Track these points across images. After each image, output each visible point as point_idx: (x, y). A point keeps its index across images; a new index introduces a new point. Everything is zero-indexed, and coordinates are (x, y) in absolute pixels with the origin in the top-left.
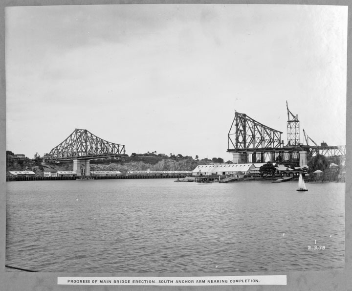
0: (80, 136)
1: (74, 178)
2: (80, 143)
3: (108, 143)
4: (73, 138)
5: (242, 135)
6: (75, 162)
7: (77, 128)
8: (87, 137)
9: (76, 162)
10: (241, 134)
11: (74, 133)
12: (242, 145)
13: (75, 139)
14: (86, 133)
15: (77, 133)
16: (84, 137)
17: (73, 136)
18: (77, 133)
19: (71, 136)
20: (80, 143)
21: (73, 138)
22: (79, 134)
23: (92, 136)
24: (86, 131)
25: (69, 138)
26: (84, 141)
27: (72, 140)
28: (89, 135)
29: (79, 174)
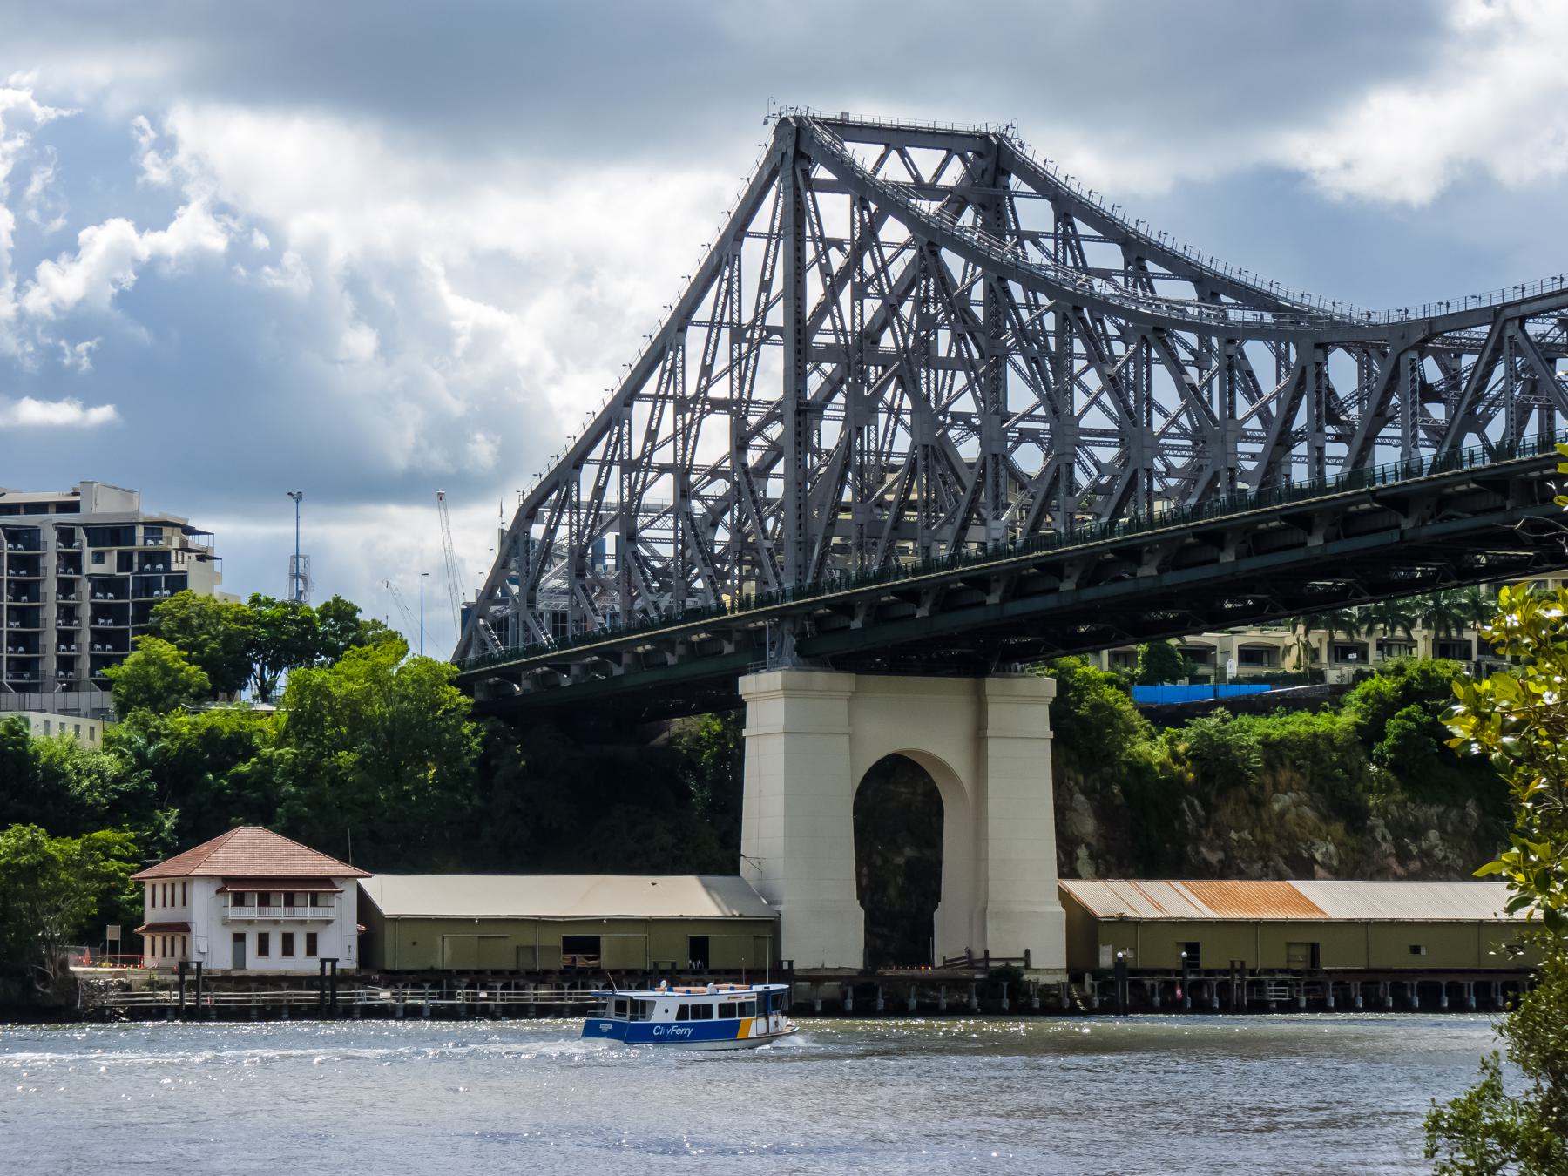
11: (763, 220)
19: (723, 258)
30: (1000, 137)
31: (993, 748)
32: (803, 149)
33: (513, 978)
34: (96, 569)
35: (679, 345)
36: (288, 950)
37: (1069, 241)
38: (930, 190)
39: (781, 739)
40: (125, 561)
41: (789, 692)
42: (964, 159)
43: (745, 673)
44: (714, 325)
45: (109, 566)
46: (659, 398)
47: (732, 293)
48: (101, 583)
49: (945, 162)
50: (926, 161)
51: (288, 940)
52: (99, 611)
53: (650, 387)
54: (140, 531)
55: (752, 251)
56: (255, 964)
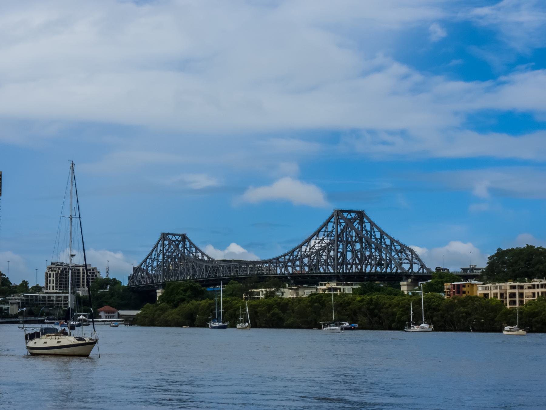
7: (166, 232)
11: (160, 243)
19: (156, 247)
25: (154, 251)
30: (185, 234)
35: (152, 254)
38: (177, 240)
42: (181, 237)
46: (150, 259)
47: (157, 250)
49: (179, 237)
50: (177, 237)
53: (149, 258)
55: (159, 245)
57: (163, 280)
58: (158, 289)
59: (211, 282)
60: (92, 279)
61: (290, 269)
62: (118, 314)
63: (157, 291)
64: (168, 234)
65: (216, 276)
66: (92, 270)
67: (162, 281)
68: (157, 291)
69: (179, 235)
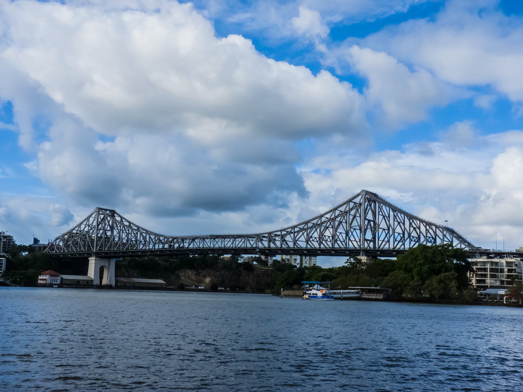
0: (103, 220)
1: (88, 285)
2: (101, 232)
3: (147, 232)
4: (91, 222)
5: (371, 228)
6: (92, 261)
8: (115, 221)
9: (94, 261)
10: (369, 227)
11: (94, 216)
12: (372, 244)
13: (95, 224)
14: (113, 216)
15: (99, 214)
16: (109, 222)
17: (91, 219)
18: (99, 214)
19: (88, 219)
20: (101, 232)
21: (91, 222)
22: (102, 216)
23: (122, 221)
24: (113, 213)
25: (85, 223)
26: (109, 228)
27: (89, 226)
28: (118, 219)
29: (96, 282)
31: (111, 266)
32: (99, 211)
33: (73, 285)
34: (4, 240)
36: (55, 281)
37: (122, 221)
39: (94, 264)
40: (7, 240)
41: (95, 260)
43: (89, 257)
44: (86, 224)
45: (5, 240)
48: (4, 242)
50: (108, 212)
51: (55, 281)
52: (3, 245)
54: (8, 237)
56: (54, 283)
57: (96, 250)
58: (91, 256)
59: (168, 252)
60: (9, 245)
61: (266, 244)
62: (62, 278)
63: (89, 258)
64: (102, 209)
65: (101, 250)
66: (8, 237)
67: (95, 250)
68: (89, 258)
69: (111, 211)
